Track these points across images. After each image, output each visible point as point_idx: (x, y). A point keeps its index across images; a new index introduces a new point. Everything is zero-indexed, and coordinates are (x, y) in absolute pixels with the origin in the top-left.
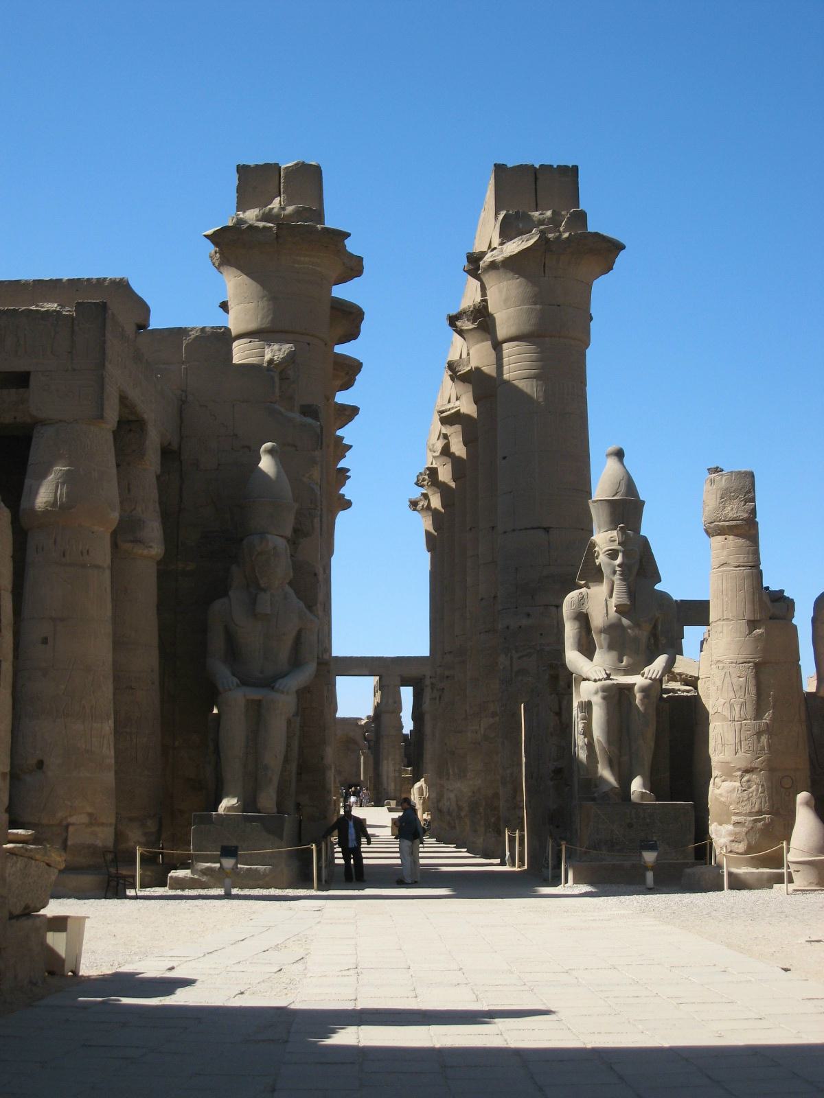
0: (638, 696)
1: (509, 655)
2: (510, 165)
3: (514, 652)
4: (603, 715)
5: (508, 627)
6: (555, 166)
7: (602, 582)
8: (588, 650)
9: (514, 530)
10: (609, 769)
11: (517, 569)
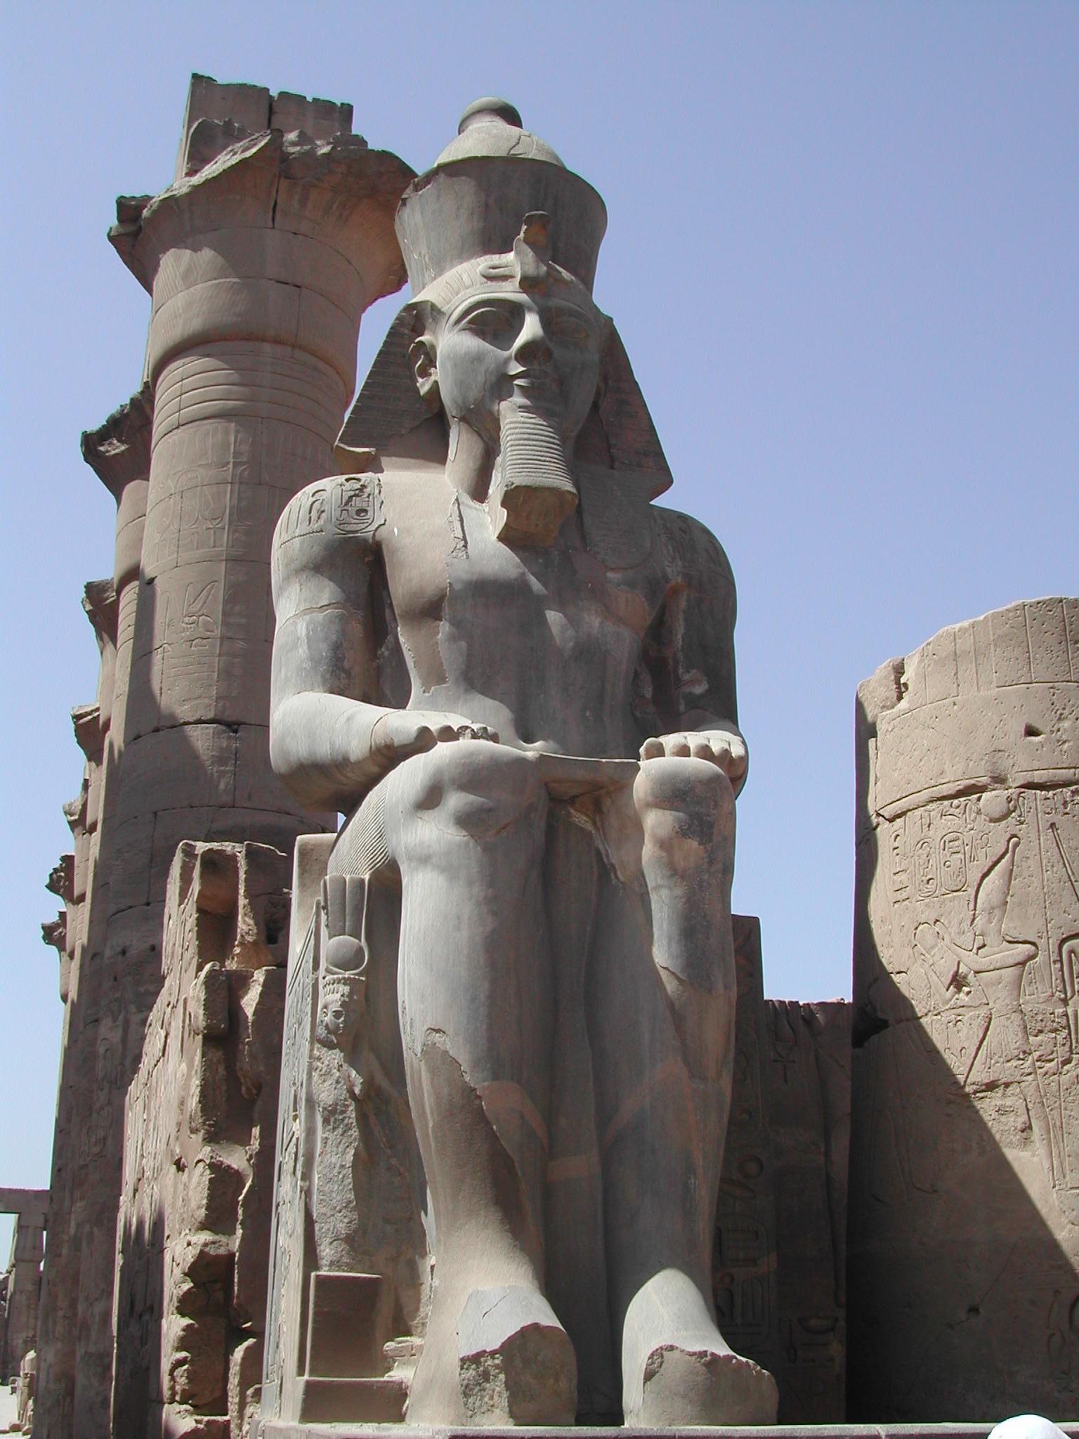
0: (656, 822)
1: (121, 1017)
2: (221, 80)
3: (133, 1008)
4: (468, 910)
5: (124, 952)
6: (309, 99)
7: (441, 459)
8: (367, 668)
9: (157, 730)
10: (495, 1216)
11: (155, 813)
